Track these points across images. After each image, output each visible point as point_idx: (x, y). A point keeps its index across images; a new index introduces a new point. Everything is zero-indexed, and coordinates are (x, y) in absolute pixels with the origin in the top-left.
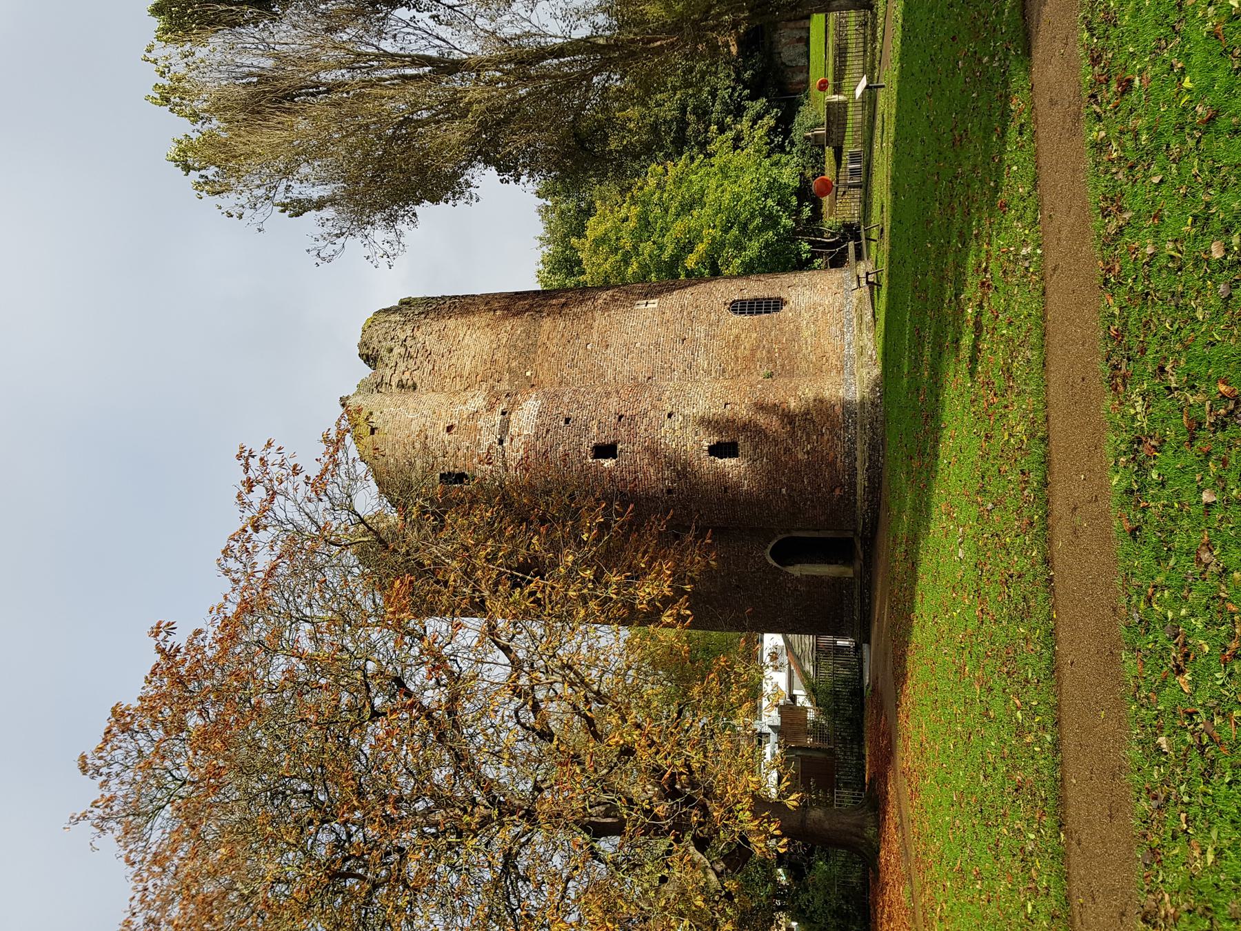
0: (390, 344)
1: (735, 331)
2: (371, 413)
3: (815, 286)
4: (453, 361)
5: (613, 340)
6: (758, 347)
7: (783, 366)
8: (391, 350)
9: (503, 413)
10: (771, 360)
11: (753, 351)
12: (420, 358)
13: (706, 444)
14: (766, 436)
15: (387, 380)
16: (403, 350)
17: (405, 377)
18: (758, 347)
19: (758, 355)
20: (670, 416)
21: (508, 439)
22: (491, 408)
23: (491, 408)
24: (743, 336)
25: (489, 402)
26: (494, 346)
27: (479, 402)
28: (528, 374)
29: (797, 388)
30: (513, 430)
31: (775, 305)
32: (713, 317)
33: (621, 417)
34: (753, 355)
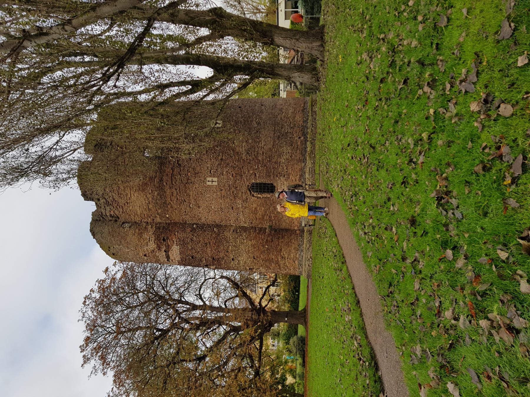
0: (97, 197)
1: (255, 206)
2: (109, 248)
3: (289, 175)
4: (131, 208)
5: (201, 203)
6: (265, 215)
7: (276, 224)
8: (99, 200)
9: (165, 251)
10: (271, 221)
11: (263, 217)
12: (115, 205)
13: (248, 268)
14: (270, 269)
15: (104, 214)
16: (105, 201)
17: (112, 213)
18: (265, 215)
19: (265, 218)
20: (233, 259)
21: (171, 261)
22: (159, 248)
23: (159, 248)
24: (258, 208)
25: (158, 244)
26: (147, 202)
27: (152, 245)
28: (167, 216)
29: (281, 250)
30: (171, 258)
31: (270, 188)
32: (244, 197)
33: (213, 258)
34: (263, 218)
